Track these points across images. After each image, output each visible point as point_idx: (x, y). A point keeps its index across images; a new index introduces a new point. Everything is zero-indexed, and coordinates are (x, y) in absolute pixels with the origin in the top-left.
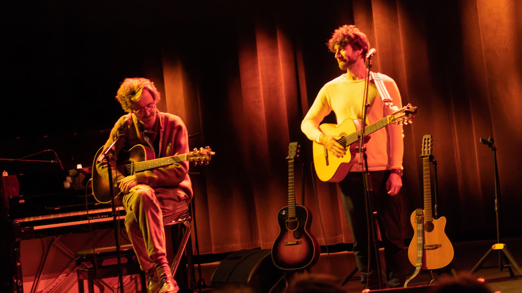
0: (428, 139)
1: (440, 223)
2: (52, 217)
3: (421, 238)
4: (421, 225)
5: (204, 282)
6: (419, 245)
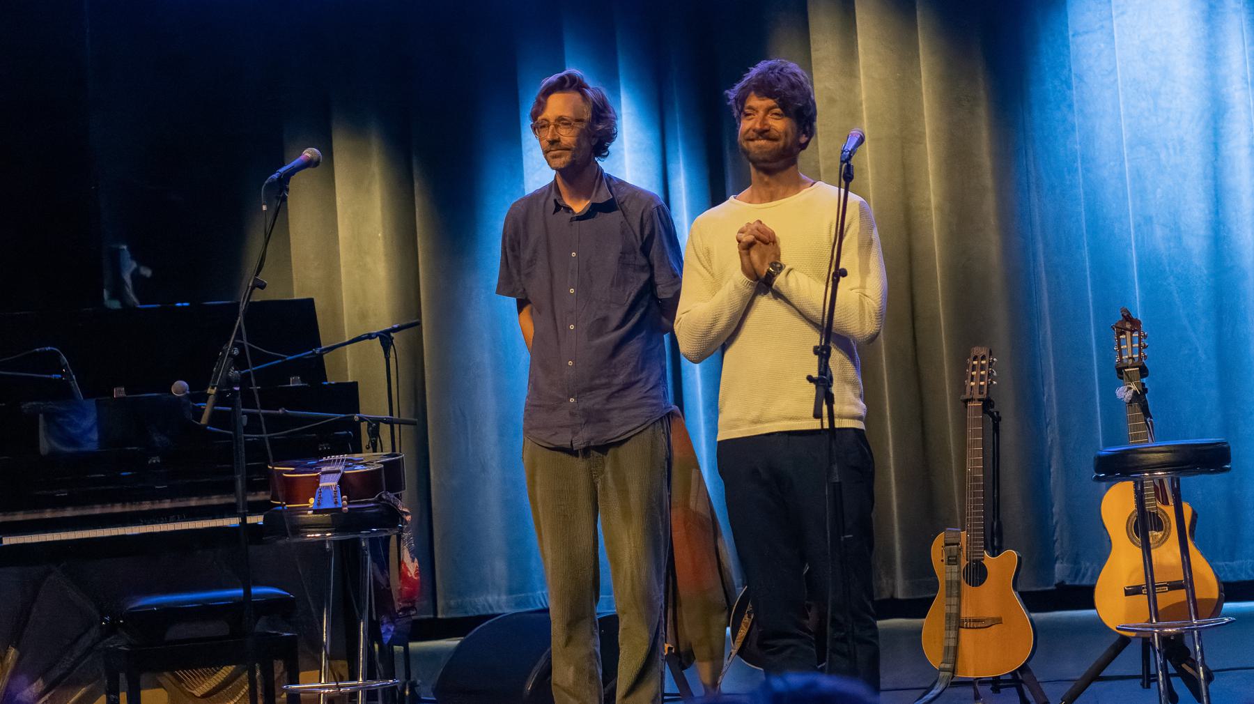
0: (983, 358)
1: (1002, 566)
2: (48, 514)
3: (954, 601)
4: (955, 568)
5: (412, 690)
6: (949, 617)
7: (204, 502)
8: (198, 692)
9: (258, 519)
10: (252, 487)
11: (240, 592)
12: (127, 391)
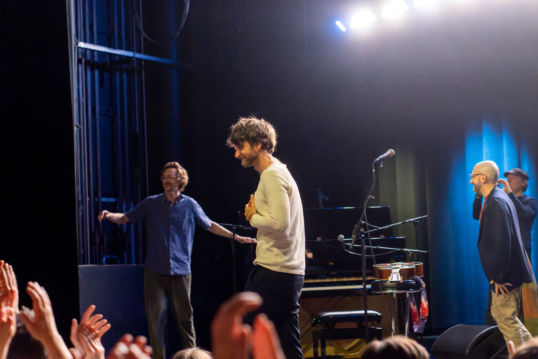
7: (348, 280)
8: (346, 348)
9: (369, 286)
10: (368, 275)
11: (363, 312)
12: (322, 239)
